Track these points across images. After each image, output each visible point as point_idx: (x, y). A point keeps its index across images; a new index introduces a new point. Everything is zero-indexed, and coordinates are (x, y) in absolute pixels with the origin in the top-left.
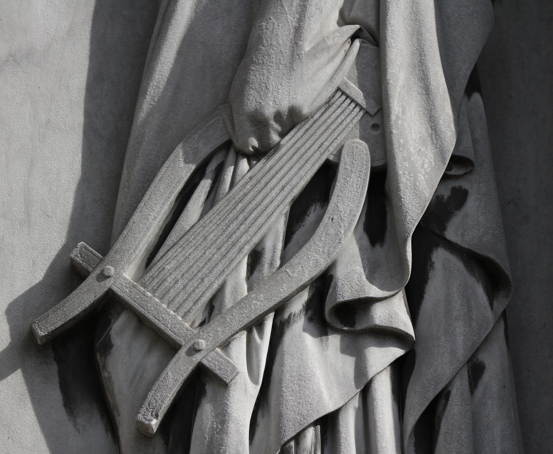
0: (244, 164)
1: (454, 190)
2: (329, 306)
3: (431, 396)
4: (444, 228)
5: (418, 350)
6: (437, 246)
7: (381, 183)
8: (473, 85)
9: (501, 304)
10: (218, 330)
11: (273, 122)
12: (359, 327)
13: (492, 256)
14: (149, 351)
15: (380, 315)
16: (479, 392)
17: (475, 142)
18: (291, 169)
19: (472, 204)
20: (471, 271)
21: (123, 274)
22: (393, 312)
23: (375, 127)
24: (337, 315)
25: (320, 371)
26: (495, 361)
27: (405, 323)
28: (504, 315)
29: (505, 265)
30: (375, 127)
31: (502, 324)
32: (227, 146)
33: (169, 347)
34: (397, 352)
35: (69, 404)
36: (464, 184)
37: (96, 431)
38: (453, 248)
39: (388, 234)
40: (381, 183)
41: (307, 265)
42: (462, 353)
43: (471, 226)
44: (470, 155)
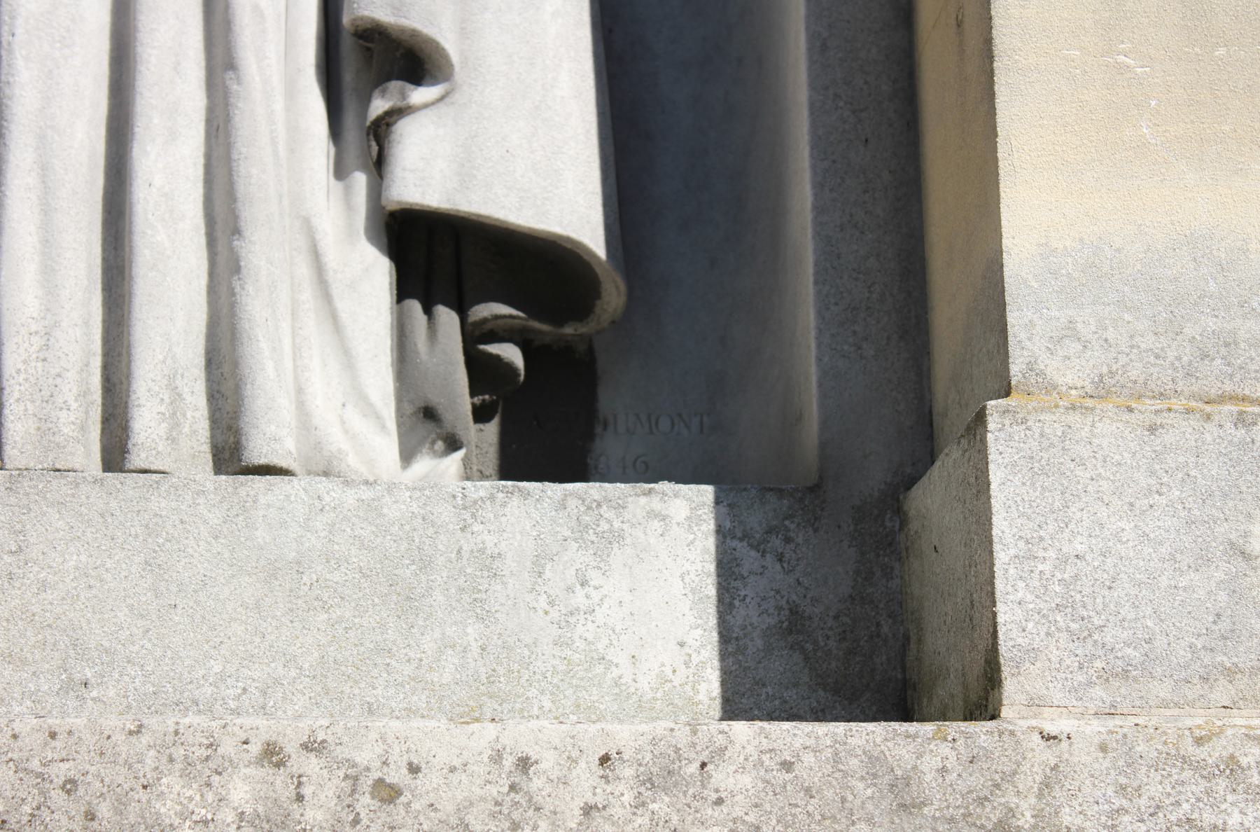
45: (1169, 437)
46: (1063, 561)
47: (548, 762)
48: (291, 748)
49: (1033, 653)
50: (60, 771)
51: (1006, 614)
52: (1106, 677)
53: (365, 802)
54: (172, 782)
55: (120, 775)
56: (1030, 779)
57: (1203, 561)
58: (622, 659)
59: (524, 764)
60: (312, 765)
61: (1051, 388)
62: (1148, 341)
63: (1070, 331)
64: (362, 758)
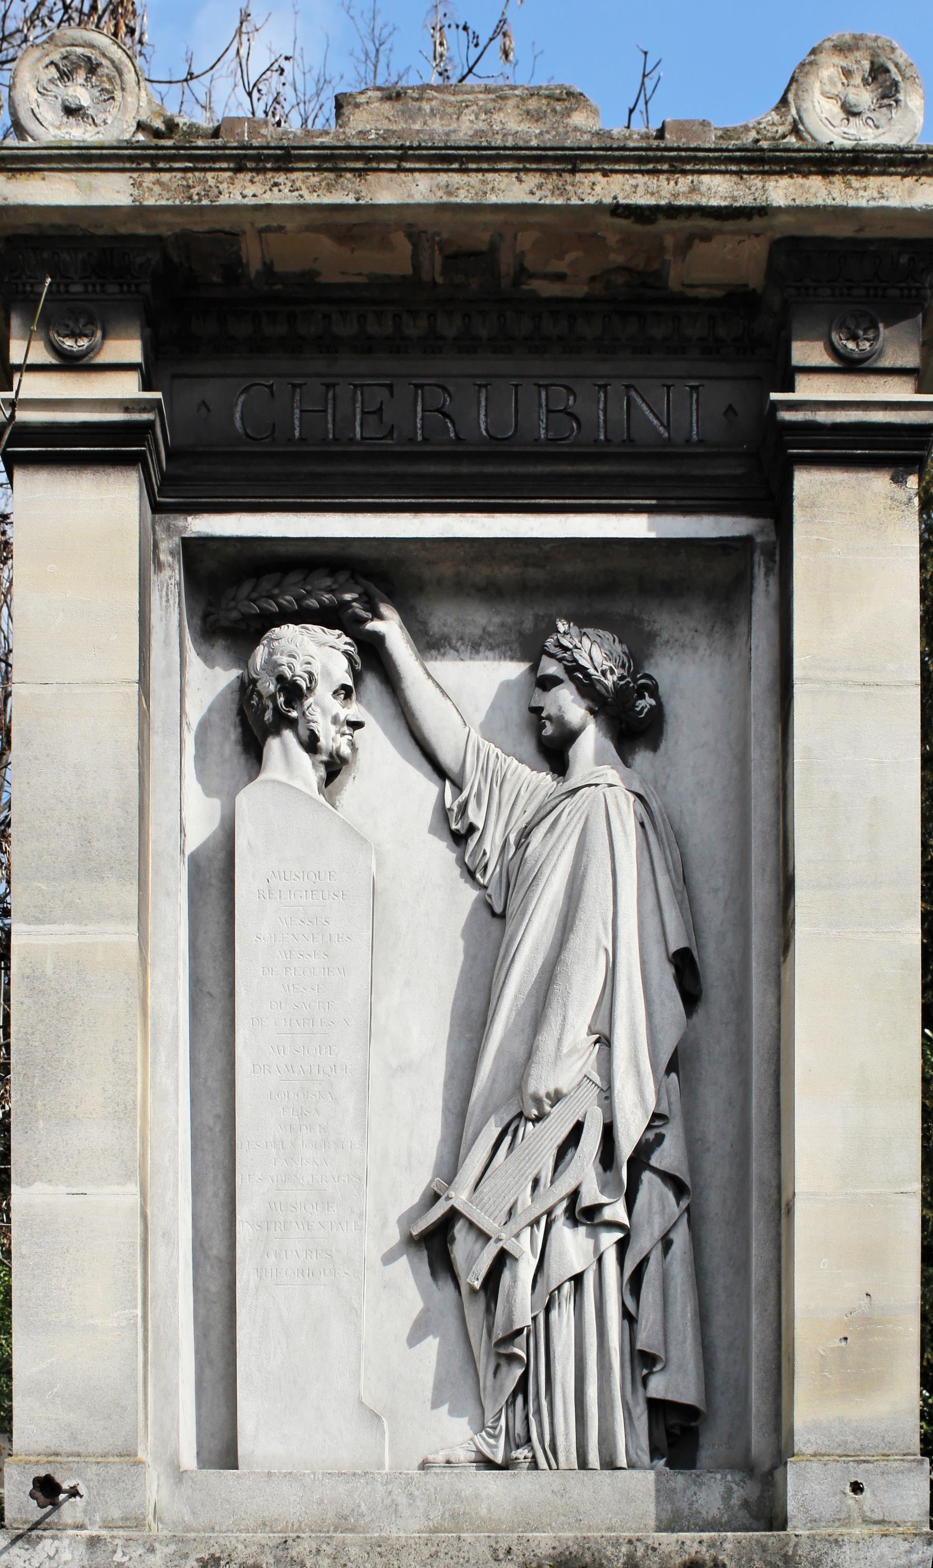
1: (657, 1135)
2: (577, 1210)
3: (638, 1261)
4: (649, 1159)
5: (632, 1234)
6: (645, 1169)
9: (684, 1204)
10: (513, 1227)
11: (545, 1099)
12: (596, 1221)
13: (677, 1174)
14: (476, 1241)
15: (608, 1214)
16: (669, 1257)
17: (670, 1104)
18: (556, 1129)
19: (667, 1143)
20: (666, 1184)
21: (460, 1197)
22: (617, 1211)
23: (606, 1098)
24: (584, 1215)
25: (573, 1248)
26: (681, 1237)
27: (624, 1219)
28: (688, 1209)
29: (687, 1180)
30: (606, 1098)
31: (686, 1215)
33: (484, 1237)
34: (619, 1235)
35: (434, 1274)
36: (662, 1130)
38: (655, 1170)
39: (614, 1164)
41: (565, 1186)
43: (668, 1156)
44: (666, 1113)
45: (829, 1466)
46: (803, 1495)
47: (688, 1542)
48: (634, 1540)
49: (795, 1516)
50: (587, 1546)
51: (789, 1508)
52: (811, 1521)
53: (650, 1552)
54: (609, 1548)
55: (600, 1547)
56: (792, 1544)
57: (835, 1494)
59: (683, 1543)
60: (639, 1544)
61: (803, 1454)
62: (827, 1443)
63: (809, 1441)
64: (650, 1542)
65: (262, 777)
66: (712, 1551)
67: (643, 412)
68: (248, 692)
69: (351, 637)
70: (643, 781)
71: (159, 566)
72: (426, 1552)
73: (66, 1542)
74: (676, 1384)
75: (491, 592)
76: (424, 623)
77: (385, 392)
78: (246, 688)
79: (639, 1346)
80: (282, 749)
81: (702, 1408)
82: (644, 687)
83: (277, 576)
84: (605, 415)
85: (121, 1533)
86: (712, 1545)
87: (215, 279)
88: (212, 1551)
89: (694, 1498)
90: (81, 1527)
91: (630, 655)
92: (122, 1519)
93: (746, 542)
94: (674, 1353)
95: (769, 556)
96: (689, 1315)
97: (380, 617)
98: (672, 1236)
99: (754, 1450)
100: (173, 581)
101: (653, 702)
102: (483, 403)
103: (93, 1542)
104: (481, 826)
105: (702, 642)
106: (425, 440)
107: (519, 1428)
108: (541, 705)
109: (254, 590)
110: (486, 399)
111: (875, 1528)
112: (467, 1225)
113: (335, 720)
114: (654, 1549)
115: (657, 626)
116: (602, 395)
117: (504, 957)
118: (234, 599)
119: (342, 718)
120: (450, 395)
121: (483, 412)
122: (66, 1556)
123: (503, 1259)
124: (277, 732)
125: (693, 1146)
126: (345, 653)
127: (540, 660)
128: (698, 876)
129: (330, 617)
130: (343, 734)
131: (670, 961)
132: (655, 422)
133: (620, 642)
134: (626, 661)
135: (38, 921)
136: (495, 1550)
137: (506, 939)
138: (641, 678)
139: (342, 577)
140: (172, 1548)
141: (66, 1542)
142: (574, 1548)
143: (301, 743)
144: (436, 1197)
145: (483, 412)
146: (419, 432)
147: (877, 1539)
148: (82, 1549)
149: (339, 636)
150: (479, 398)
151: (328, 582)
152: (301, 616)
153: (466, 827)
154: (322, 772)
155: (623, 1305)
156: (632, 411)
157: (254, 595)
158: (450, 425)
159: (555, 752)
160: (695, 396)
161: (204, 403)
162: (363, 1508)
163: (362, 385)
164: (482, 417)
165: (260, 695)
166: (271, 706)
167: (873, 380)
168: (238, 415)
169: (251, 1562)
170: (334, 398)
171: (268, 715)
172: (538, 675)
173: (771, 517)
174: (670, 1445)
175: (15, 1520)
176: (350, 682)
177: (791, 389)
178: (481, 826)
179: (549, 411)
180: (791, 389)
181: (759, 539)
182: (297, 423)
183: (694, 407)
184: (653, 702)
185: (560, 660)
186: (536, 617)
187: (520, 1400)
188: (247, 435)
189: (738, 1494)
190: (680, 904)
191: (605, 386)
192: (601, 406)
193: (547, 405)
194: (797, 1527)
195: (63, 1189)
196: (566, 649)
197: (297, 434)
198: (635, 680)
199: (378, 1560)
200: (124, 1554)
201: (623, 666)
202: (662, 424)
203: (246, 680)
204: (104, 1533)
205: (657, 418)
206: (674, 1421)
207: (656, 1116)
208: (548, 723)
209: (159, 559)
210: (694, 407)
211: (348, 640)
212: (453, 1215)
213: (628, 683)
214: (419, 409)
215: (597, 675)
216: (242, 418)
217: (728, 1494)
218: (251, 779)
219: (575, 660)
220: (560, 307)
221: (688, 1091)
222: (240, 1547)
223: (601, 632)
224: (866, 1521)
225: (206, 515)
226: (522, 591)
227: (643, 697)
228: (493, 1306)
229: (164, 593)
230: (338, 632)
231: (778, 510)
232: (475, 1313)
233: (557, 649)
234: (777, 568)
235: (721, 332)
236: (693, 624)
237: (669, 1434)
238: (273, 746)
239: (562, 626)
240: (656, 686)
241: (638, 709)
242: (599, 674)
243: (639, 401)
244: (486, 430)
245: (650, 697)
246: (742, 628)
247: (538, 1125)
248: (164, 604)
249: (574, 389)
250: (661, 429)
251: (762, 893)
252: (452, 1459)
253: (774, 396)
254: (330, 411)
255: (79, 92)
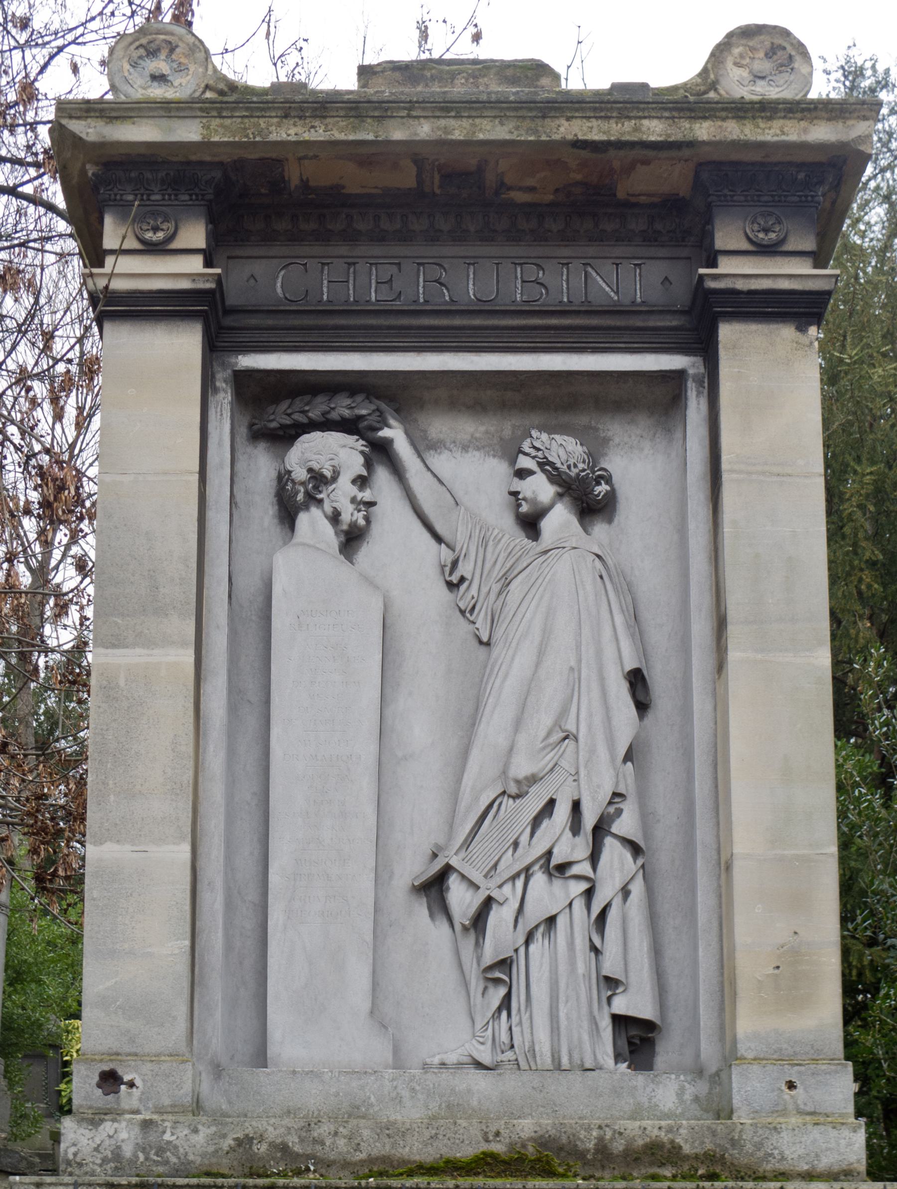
0: (511, 801)
1: (616, 809)
2: (552, 865)
3: (602, 906)
4: (610, 827)
5: (597, 885)
6: (607, 835)
7: (576, 806)
8: (628, 757)
12: (567, 875)
13: (634, 839)
14: (467, 890)
17: (627, 786)
19: (625, 815)
20: (624, 846)
22: (584, 868)
23: (575, 780)
26: (637, 888)
29: (642, 844)
30: (575, 780)
31: (641, 871)
32: (504, 793)
36: (621, 806)
37: (445, 926)
38: (616, 836)
39: (582, 831)
40: (576, 806)
42: (618, 885)
43: (626, 824)
44: (624, 792)
45: (767, 1068)
46: (746, 1092)
47: (649, 1128)
48: (603, 1126)
49: (739, 1108)
50: (563, 1130)
51: (734, 1101)
52: (753, 1112)
53: (617, 1136)
54: (582, 1132)
55: (574, 1131)
56: (738, 1130)
57: (773, 1091)
58: (661, 1105)
59: (645, 1129)
60: (607, 1129)
61: (745, 1059)
62: (765, 1049)
63: (750, 1048)
64: (616, 1128)
65: (294, 541)
66: (670, 1136)
67: (598, 283)
68: (284, 480)
69: (366, 441)
70: (601, 545)
71: (216, 390)
72: (427, 1134)
73: (124, 1124)
74: (636, 1002)
75: (477, 408)
76: (425, 431)
77: (395, 269)
78: (283, 478)
79: (605, 972)
80: (312, 523)
81: (658, 1021)
82: (601, 477)
83: (307, 398)
84: (568, 284)
85: (170, 1117)
86: (670, 1130)
87: (263, 191)
88: (247, 1132)
89: (653, 1094)
90: (137, 1112)
91: (590, 454)
92: (171, 1106)
93: (679, 375)
94: (633, 979)
95: (699, 382)
96: (646, 949)
97: (389, 426)
98: (631, 887)
99: (703, 1056)
100: (226, 401)
101: (608, 488)
102: (471, 276)
103: (146, 1125)
104: (470, 578)
105: (647, 445)
106: (426, 301)
107: (504, 1037)
108: (519, 489)
109: (289, 407)
110: (474, 273)
111: (808, 1118)
112: (459, 878)
113: (353, 500)
114: (620, 1134)
115: (610, 434)
116: (565, 270)
117: (490, 675)
118: (273, 414)
119: (359, 498)
120: (445, 270)
121: (471, 282)
122: (124, 1135)
123: (489, 902)
124: (307, 508)
125: (646, 817)
126: (362, 452)
127: (517, 457)
128: (646, 615)
129: (348, 426)
130: (359, 511)
131: (625, 678)
132: (607, 289)
133: (581, 444)
134: (586, 457)
135: (114, 646)
136: (486, 1133)
137: (492, 660)
138: (599, 470)
139: (359, 398)
140: (214, 1129)
141: (124, 1124)
142: (553, 1132)
143: (326, 517)
144: (435, 856)
145: (471, 282)
146: (421, 296)
147: (810, 1127)
148: (137, 1130)
149: (357, 440)
150: (468, 272)
151: (348, 402)
152: (326, 425)
153: (458, 578)
154: (342, 538)
155: (590, 940)
156: (589, 281)
157: (289, 411)
158: (445, 291)
159: (530, 523)
160: (638, 271)
161: (252, 275)
162: (373, 1099)
163: (376, 264)
164: (471, 286)
165: (293, 481)
166: (302, 490)
167: (779, 260)
168: (279, 285)
169: (279, 1141)
170: (354, 272)
171: (300, 497)
172: (517, 467)
173: (701, 356)
174: (631, 1052)
175: (81, 1106)
176: (365, 473)
177: (714, 265)
178: (470, 578)
179: (523, 282)
180: (714, 265)
181: (691, 371)
182: (325, 290)
183: (638, 278)
184: (608, 488)
185: (534, 457)
186: (514, 426)
187: (504, 1014)
188: (286, 298)
189: (690, 1091)
190: (633, 635)
191: (568, 264)
192: (565, 277)
193: (522, 277)
194: (742, 1116)
195: (128, 847)
196: (538, 449)
197: (325, 297)
198: (593, 473)
199: (387, 1140)
200: (173, 1134)
201: (584, 462)
202: (612, 290)
203: (283, 472)
204: (155, 1117)
205: (609, 286)
206: (634, 1032)
207: (615, 795)
208: (523, 503)
209: (215, 385)
210: (638, 278)
211: (364, 443)
212: (447, 870)
213: (588, 474)
214: (421, 280)
215: (564, 468)
216: (282, 287)
217: (680, 1093)
218: (285, 543)
219: (545, 458)
220: (530, 209)
221: (641, 775)
222: (271, 1129)
223: (566, 438)
224: (801, 1113)
225: (253, 355)
226: (503, 407)
227: (600, 484)
228: (481, 941)
229: (219, 410)
230: (356, 437)
231: (706, 347)
232: (467, 944)
233: (532, 450)
234: (706, 391)
235: (658, 226)
236: (639, 432)
237: (630, 1043)
238: (303, 520)
239: (535, 433)
240: (611, 476)
241: (596, 493)
242: (565, 467)
243: (594, 274)
244: (474, 295)
245: (607, 483)
246: (678, 435)
247: (518, 801)
248: (219, 417)
249: (544, 266)
250: (612, 294)
251: (701, 628)
252: (447, 1062)
253: (702, 271)
254: (351, 282)
255: (160, 65)
